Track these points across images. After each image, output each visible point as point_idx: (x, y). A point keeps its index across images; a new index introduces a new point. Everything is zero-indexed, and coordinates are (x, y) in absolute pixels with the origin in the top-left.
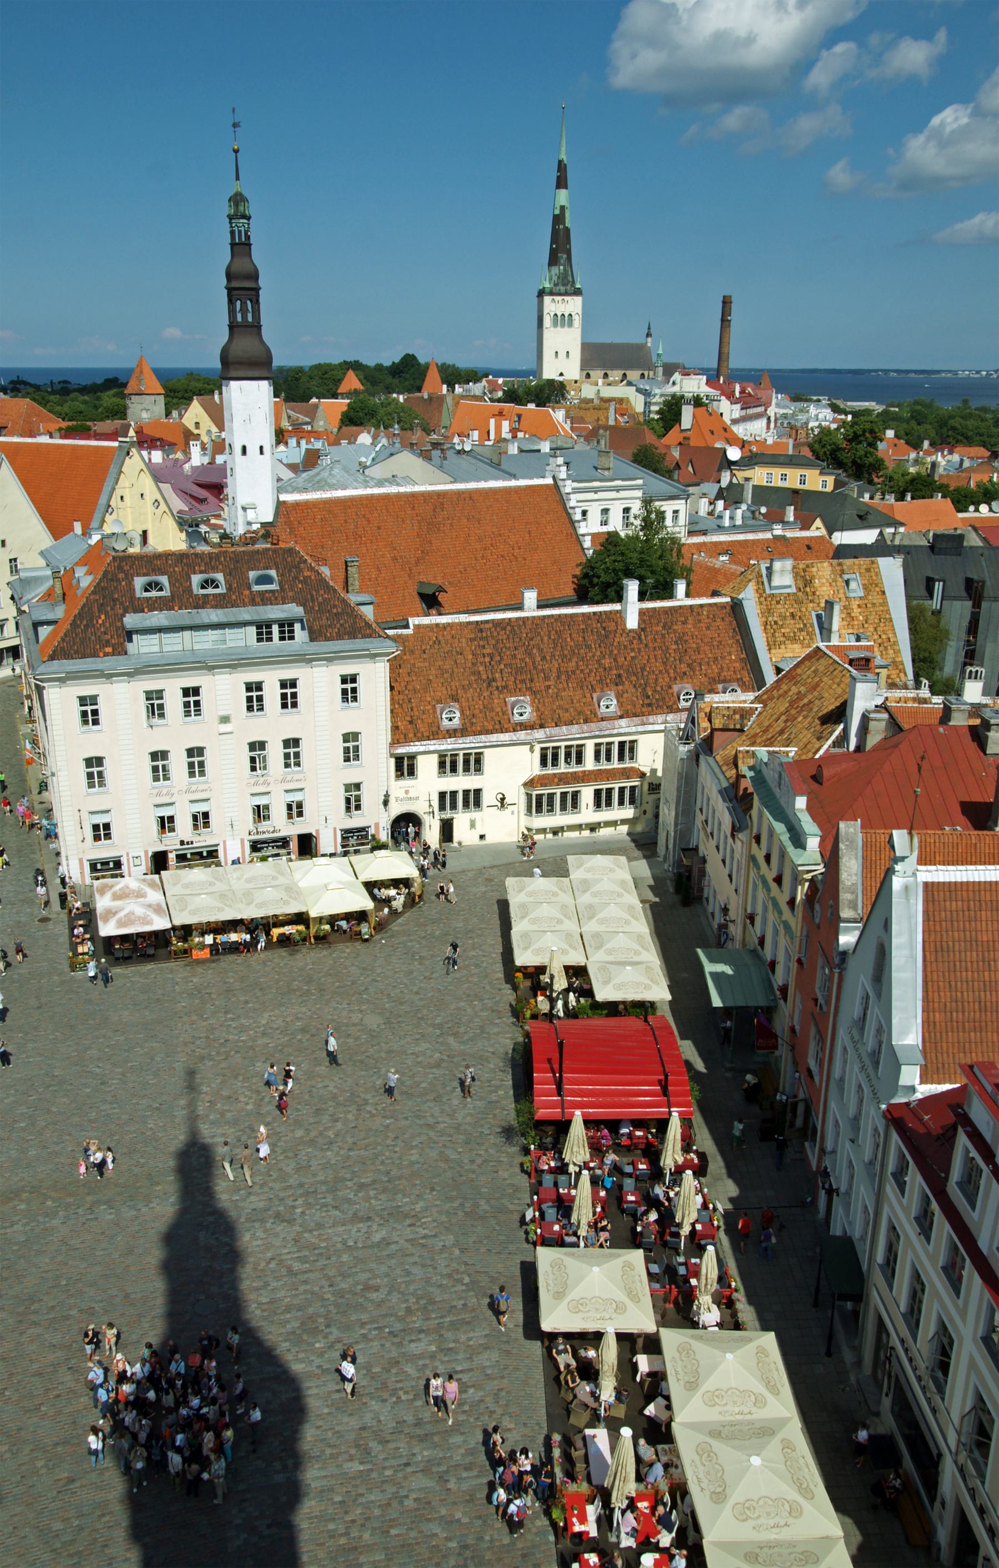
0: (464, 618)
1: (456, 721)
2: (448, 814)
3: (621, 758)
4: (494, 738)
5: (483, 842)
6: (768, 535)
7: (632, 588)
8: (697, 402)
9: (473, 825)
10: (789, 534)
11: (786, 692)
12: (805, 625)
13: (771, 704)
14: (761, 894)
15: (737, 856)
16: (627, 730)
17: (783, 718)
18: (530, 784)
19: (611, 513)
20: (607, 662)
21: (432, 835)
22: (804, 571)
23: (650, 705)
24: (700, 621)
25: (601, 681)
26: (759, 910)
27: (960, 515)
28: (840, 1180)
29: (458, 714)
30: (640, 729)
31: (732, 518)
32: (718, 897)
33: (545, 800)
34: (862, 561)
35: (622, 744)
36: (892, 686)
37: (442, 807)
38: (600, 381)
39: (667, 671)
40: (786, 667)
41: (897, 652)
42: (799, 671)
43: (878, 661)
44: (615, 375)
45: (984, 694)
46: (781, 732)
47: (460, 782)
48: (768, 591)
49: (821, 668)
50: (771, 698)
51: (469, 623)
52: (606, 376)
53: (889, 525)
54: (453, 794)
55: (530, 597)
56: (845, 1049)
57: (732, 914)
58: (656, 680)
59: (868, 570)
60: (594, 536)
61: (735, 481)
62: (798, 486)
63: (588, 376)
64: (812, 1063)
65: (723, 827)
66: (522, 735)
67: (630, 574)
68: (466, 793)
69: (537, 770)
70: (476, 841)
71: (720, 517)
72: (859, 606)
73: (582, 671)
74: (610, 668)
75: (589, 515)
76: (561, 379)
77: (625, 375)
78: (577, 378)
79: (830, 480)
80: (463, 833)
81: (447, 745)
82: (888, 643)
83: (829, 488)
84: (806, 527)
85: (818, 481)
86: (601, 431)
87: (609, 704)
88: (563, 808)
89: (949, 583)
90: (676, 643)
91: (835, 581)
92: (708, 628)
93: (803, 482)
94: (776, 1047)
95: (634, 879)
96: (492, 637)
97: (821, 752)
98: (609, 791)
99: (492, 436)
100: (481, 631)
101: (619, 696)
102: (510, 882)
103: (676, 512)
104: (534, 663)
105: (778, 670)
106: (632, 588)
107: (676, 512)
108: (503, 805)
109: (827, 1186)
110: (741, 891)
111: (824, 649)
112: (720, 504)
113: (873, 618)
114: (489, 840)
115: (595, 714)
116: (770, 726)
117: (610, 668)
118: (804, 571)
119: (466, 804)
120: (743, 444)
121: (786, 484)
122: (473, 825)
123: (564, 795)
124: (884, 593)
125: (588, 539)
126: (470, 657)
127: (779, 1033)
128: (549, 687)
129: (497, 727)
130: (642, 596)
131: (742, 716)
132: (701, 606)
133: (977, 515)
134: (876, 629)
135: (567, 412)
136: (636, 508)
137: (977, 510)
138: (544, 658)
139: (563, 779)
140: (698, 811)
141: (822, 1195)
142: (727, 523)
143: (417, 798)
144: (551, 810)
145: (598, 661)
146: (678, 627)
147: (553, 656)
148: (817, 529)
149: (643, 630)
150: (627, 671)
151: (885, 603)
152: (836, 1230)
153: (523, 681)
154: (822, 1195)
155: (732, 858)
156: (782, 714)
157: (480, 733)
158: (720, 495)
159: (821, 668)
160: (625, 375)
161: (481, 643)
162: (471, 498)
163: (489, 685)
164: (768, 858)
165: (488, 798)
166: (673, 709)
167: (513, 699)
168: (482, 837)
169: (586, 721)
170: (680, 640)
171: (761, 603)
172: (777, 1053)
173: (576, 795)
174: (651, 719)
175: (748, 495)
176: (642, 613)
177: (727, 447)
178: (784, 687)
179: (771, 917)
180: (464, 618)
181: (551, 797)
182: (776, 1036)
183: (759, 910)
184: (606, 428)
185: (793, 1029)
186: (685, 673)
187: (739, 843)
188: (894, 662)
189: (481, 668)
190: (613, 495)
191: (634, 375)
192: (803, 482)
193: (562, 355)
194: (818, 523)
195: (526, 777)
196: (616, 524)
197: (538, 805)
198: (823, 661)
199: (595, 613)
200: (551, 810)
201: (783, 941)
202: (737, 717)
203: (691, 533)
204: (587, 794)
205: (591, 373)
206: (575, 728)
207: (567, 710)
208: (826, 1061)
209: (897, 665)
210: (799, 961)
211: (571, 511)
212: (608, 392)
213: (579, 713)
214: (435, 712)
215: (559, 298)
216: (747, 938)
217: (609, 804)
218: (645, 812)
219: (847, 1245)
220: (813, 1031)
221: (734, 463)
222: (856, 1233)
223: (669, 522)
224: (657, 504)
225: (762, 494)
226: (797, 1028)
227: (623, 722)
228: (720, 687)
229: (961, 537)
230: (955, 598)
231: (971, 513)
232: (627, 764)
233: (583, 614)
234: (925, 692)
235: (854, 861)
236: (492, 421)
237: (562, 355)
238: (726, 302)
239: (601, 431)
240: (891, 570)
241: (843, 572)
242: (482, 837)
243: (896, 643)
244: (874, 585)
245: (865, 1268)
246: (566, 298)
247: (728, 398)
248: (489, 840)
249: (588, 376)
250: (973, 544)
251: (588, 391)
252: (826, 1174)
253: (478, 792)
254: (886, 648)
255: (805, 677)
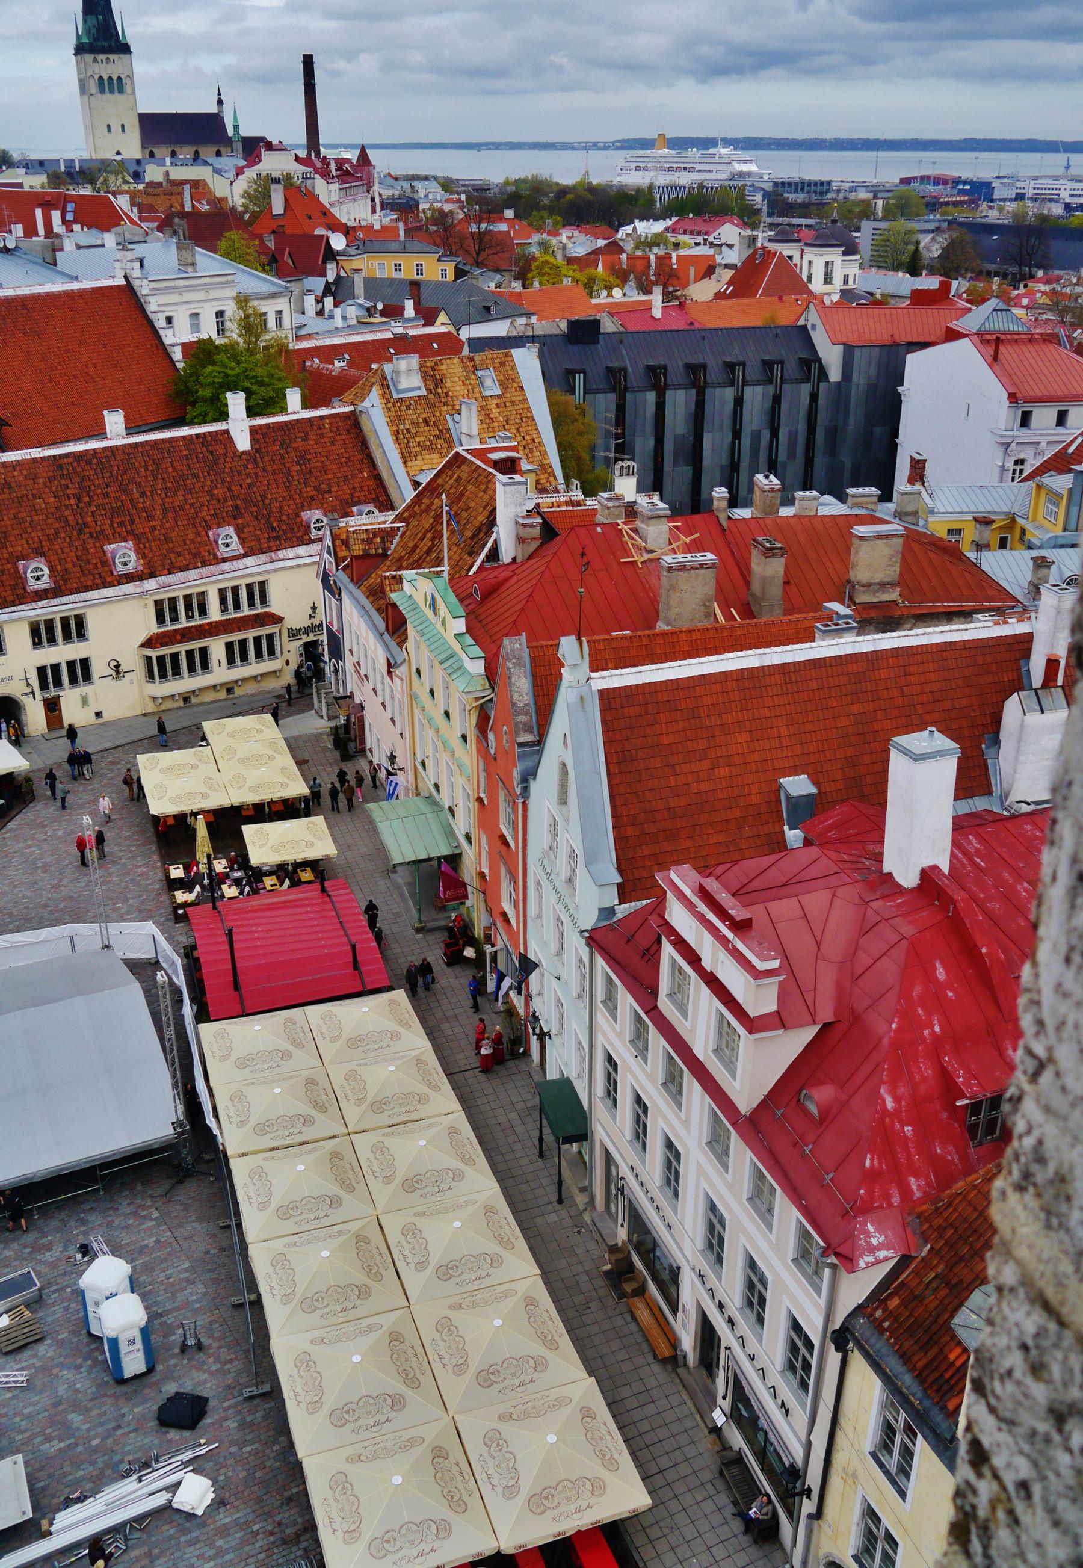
0: (36, 453)
1: (46, 582)
2: (52, 692)
3: (251, 604)
4: (94, 594)
5: (101, 721)
6: (388, 335)
7: (236, 402)
8: (287, 181)
9: (85, 702)
10: (412, 332)
11: (429, 507)
12: (441, 431)
13: (414, 523)
14: (430, 734)
15: (397, 696)
16: (254, 570)
17: (429, 535)
18: (149, 643)
19: (201, 317)
20: (219, 492)
21: (35, 716)
22: (433, 369)
23: (277, 538)
24: (322, 436)
25: (215, 516)
26: (430, 751)
27: (594, 301)
28: (548, 1021)
29: (46, 571)
30: (269, 567)
31: (344, 318)
32: (383, 745)
33: (168, 661)
34: (497, 354)
35: (249, 587)
36: (542, 490)
37: (44, 686)
38: (168, 160)
39: (292, 497)
40: (424, 479)
41: (544, 454)
42: (440, 481)
43: (525, 466)
44: (185, 153)
45: (638, 491)
46: (429, 552)
47: (62, 653)
48: (395, 396)
49: (465, 476)
50: (413, 515)
51: (43, 459)
52: (173, 154)
53: (520, 315)
54: (56, 668)
55: (115, 421)
56: (539, 883)
57: (400, 762)
58: (281, 507)
59: (502, 364)
60: (186, 347)
61: (343, 274)
62: (416, 277)
63: (152, 155)
64: (507, 907)
65: (378, 666)
66: (128, 588)
67: (234, 387)
68: (71, 664)
69: (154, 629)
70: (92, 719)
71: (331, 317)
72: (497, 405)
73: (191, 505)
74: (225, 499)
75: (175, 321)
76: (119, 158)
77: (196, 152)
78: (139, 156)
79: (450, 268)
80: (73, 711)
81: (39, 611)
82: (532, 445)
83: (451, 276)
84: (430, 321)
85: (436, 269)
86: (176, 220)
87: (228, 538)
88: (191, 669)
89: (589, 375)
90: (298, 463)
91: (468, 378)
92: (333, 443)
93: (420, 272)
94: (466, 897)
95: (286, 739)
96: (75, 472)
97: (474, 569)
98: (243, 643)
99: (41, 231)
100: (60, 467)
101: (239, 531)
102: (141, 759)
103: (279, 313)
104: (132, 500)
105: (416, 484)
106: (236, 402)
107: (279, 313)
108: (118, 673)
109: (538, 1031)
110: (407, 734)
111: (464, 454)
112: (329, 301)
113: (514, 418)
114: (107, 716)
115: (215, 555)
116: (416, 546)
117: (225, 499)
118: (433, 369)
119: (73, 680)
120: (347, 231)
121: (401, 275)
122: (85, 702)
123: (190, 654)
124: (522, 388)
125: (178, 349)
126: (52, 500)
127: (467, 880)
128: (154, 528)
129: (98, 581)
130: (251, 412)
131: (382, 538)
132: (322, 418)
133: (610, 300)
134: (518, 429)
135: (132, 199)
136: (231, 309)
137: (610, 295)
138: (143, 494)
139: (186, 635)
140: (347, 653)
141: (534, 1039)
142: (338, 322)
143: (10, 678)
144: (177, 673)
145: (210, 493)
146: (299, 443)
147: (153, 491)
148: (441, 326)
149: (257, 451)
150: (245, 501)
151: (525, 401)
152: (552, 1074)
153: (122, 524)
154: (534, 1039)
155: (393, 698)
156: (427, 531)
157: (78, 591)
158: (328, 290)
159: (465, 476)
160: (196, 152)
161: (63, 482)
162: (24, 307)
163: (80, 532)
164: (432, 692)
165: (98, 669)
166: (304, 539)
167: (113, 546)
168: (98, 715)
169: (205, 564)
170: (303, 458)
171: (389, 410)
172: (468, 903)
173: (204, 652)
174: (281, 554)
175: (359, 288)
176: (253, 431)
177: (330, 234)
178: (426, 501)
179: (445, 757)
180: (36, 453)
181: (175, 657)
182: (464, 885)
183: (430, 751)
184: (183, 215)
185: (482, 875)
186: (312, 498)
187: (396, 680)
188: (542, 466)
189: (67, 513)
190: (200, 295)
191: (207, 152)
192: (420, 272)
193: (116, 128)
194: (442, 318)
195: (142, 638)
196: (208, 330)
197: (160, 669)
198: (464, 467)
199: (198, 436)
200: (177, 673)
201: (460, 781)
202: (378, 540)
203: (299, 338)
204: (217, 648)
205: (156, 151)
206: (193, 574)
207: (179, 554)
208: (521, 902)
209: (545, 468)
210: (479, 800)
211: (152, 316)
212: (179, 173)
213: (195, 556)
214: (17, 571)
215: (101, 57)
216: (420, 785)
217: (244, 658)
218: (287, 663)
219: (565, 1085)
220: (503, 871)
221: (339, 253)
222: (572, 1073)
223: (271, 323)
224: (255, 303)
225: (373, 286)
226: (486, 871)
227: (249, 561)
228: (355, 509)
229: (597, 323)
230: (598, 391)
231: (603, 298)
232: (259, 610)
233: (184, 438)
234: (577, 495)
235: (523, 680)
236: (39, 212)
237: (116, 128)
238: (308, 62)
239: (176, 220)
240: (527, 363)
241: (475, 368)
242: (98, 715)
243: (541, 444)
244: (509, 380)
245: (586, 1106)
246: (112, 57)
247: (323, 176)
248: (107, 716)
249: (152, 155)
250: (610, 330)
251: (153, 173)
252: (536, 1018)
253: (85, 663)
254: (531, 450)
255: (447, 487)
